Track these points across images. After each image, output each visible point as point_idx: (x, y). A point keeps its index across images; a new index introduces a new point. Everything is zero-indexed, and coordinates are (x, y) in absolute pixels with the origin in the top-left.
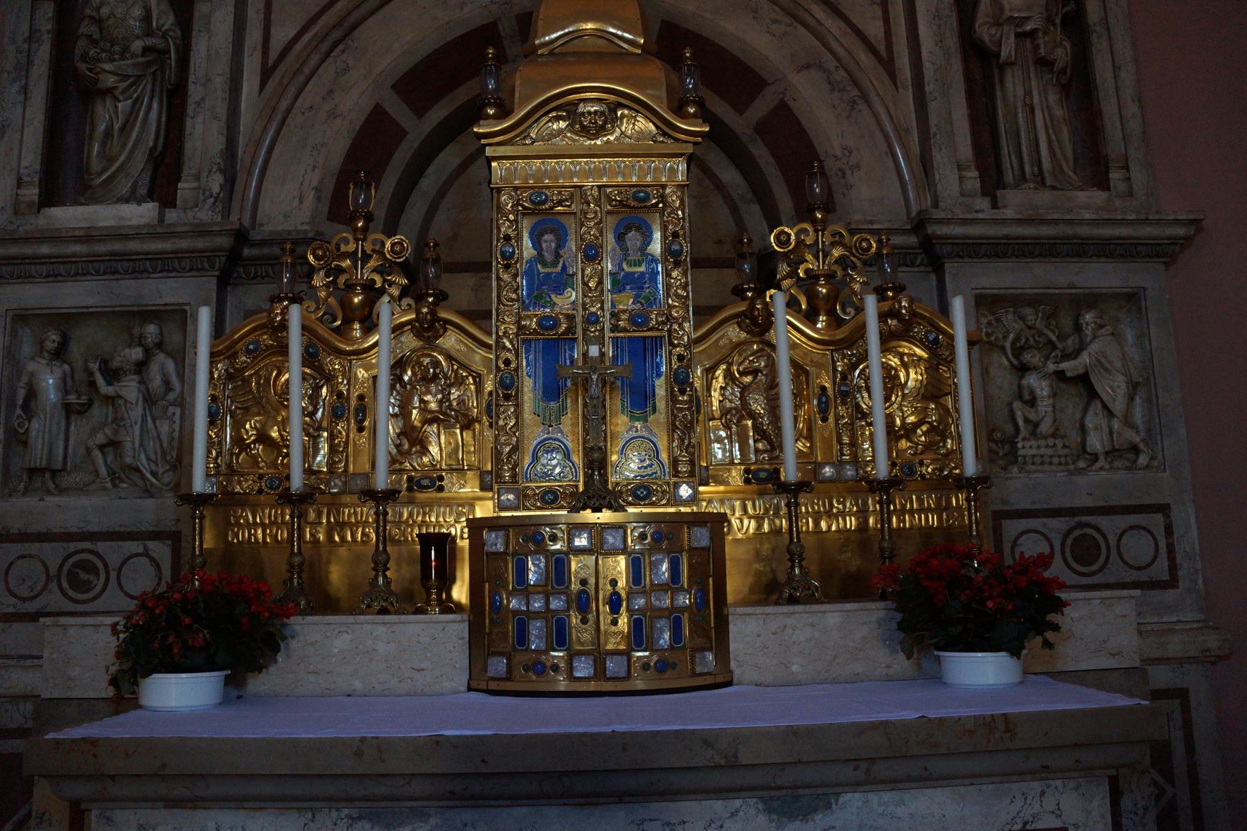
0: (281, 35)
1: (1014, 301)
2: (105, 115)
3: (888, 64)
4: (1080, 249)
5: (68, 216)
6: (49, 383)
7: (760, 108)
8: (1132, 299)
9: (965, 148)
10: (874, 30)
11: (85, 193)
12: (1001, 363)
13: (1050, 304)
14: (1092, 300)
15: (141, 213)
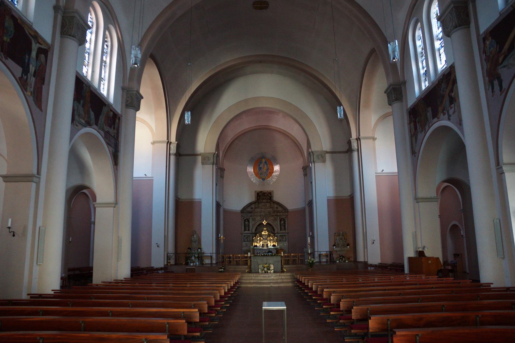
0: (253, 223)
1: (281, 235)
2: (246, 228)
3: (277, 225)
4: (284, 233)
5: (245, 232)
6: (245, 238)
7: (272, 226)
8: (286, 235)
9: (280, 229)
10: (277, 223)
11: (246, 231)
12: (281, 237)
13: (283, 235)
14: (285, 235)
15: (248, 232)
